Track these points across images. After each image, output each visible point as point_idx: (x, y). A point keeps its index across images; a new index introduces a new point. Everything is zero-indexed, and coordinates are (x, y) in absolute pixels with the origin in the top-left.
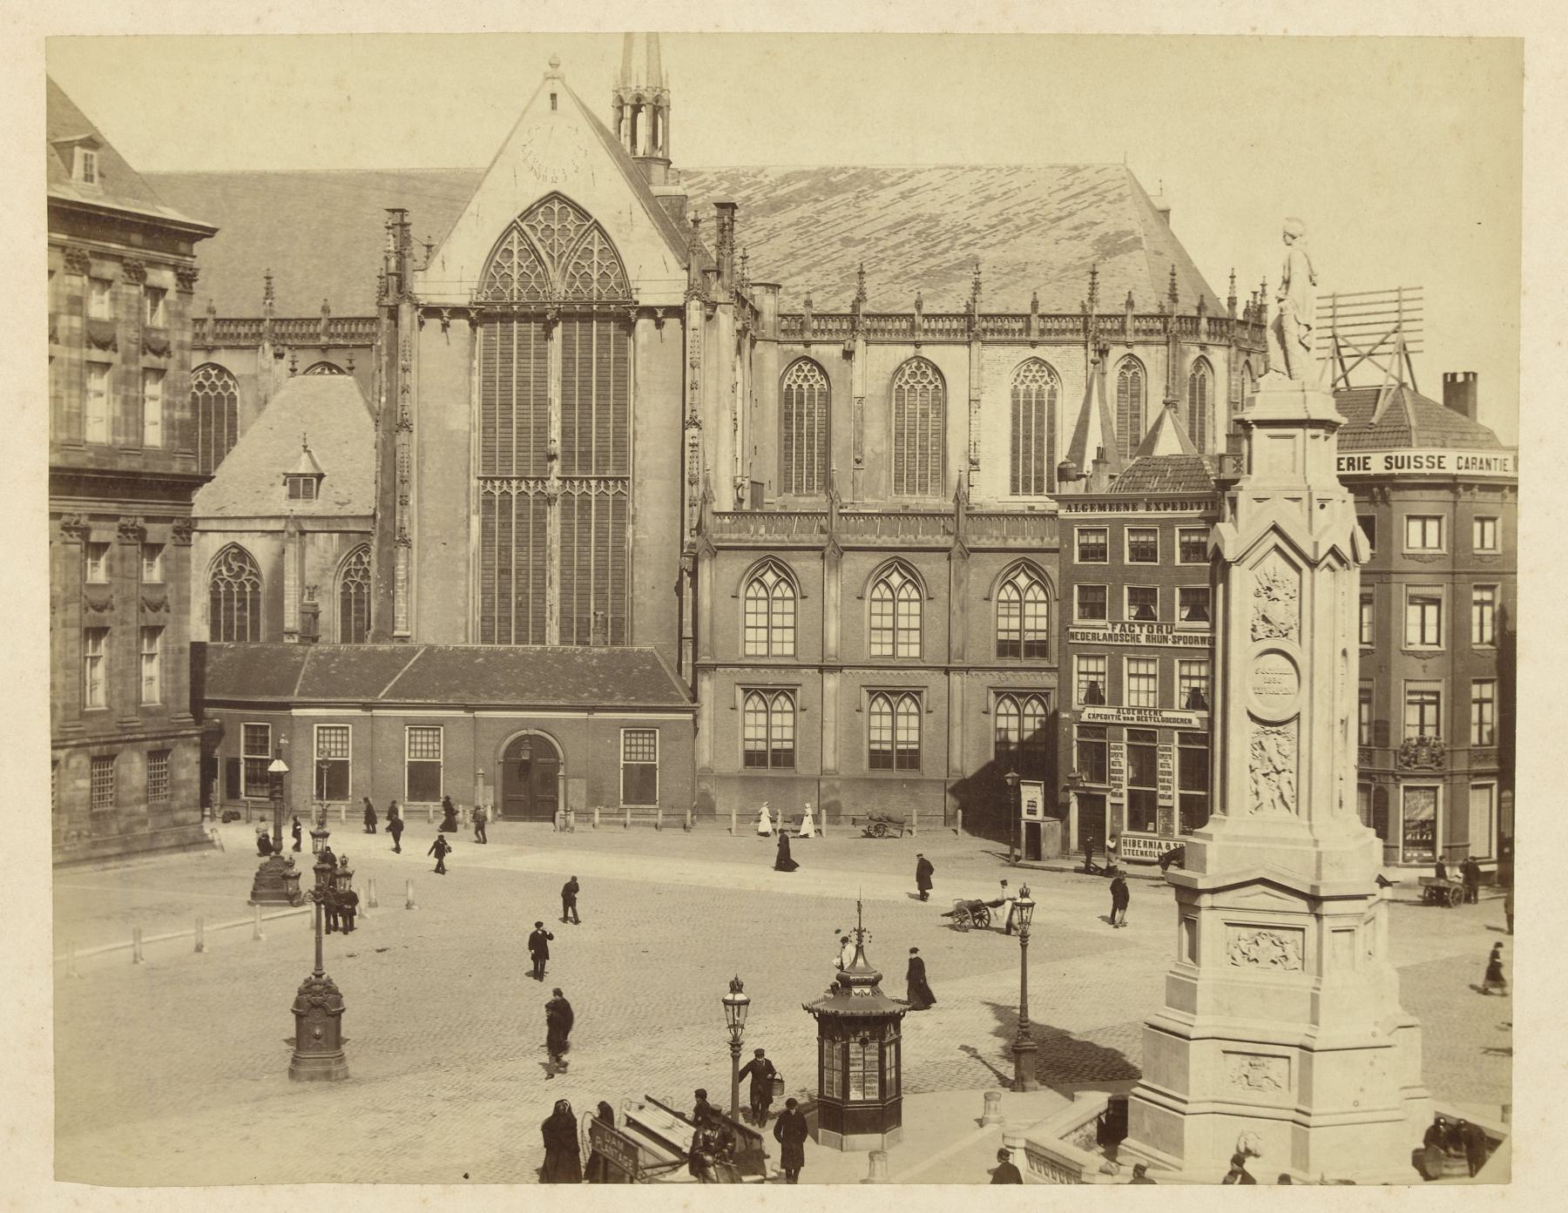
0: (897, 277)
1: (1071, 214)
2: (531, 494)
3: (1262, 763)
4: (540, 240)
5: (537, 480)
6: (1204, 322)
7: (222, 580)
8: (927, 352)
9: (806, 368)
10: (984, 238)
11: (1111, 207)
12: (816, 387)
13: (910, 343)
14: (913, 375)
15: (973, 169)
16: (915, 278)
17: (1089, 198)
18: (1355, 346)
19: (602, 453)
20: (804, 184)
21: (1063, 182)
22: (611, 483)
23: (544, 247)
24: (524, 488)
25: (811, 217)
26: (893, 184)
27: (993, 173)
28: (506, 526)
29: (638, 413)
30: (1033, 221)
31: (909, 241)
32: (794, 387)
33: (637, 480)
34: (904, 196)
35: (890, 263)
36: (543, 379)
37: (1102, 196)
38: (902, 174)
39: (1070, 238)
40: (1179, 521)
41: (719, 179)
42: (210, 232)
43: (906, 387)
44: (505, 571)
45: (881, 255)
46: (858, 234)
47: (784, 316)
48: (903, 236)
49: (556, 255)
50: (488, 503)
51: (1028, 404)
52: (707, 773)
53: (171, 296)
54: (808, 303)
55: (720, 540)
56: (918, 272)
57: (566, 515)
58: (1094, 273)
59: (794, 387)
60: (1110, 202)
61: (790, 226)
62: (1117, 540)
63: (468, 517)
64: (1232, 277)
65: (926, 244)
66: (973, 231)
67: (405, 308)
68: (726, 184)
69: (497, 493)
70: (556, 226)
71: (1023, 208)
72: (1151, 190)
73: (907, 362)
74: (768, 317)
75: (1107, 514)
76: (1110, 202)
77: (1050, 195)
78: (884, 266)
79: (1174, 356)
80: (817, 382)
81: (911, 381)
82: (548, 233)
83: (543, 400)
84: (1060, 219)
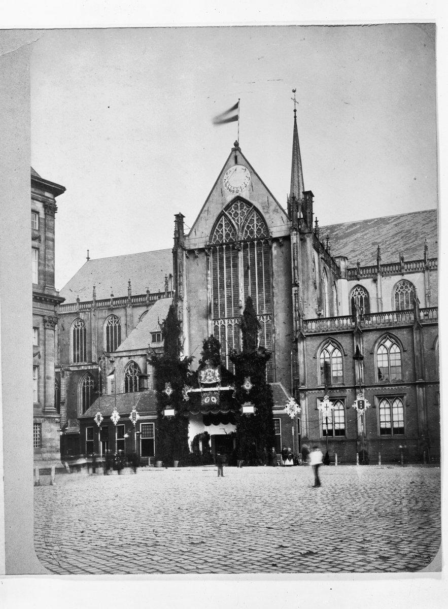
0: (395, 252)
4: (233, 218)
7: (129, 376)
9: (359, 290)
12: (363, 296)
23: (235, 221)
24: (230, 323)
26: (392, 222)
31: (398, 240)
41: (326, 230)
47: (349, 270)
49: (239, 224)
52: (306, 440)
65: (405, 240)
68: (329, 231)
69: (219, 326)
74: (343, 270)
78: (389, 250)
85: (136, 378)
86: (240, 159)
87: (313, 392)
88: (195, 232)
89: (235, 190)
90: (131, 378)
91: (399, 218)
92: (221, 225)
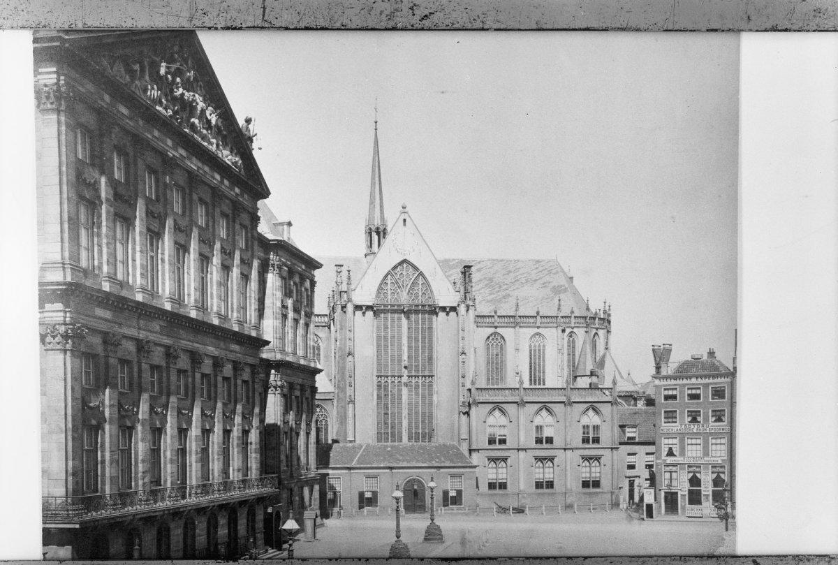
5: (398, 376)
8: (499, 330)
17: (546, 272)
19: (424, 366)
29: (438, 350)
31: (483, 288)
36: (400, 337)
37: (550, 272)
40: (711, 384)
44: (386, 414)
50: (379, 386)
62: (682, 392)
66: (506, 284)
72: (566, 270)
75: (678, 382)
83: (400, 345)
84: (536, 280)
91: (479, 263)
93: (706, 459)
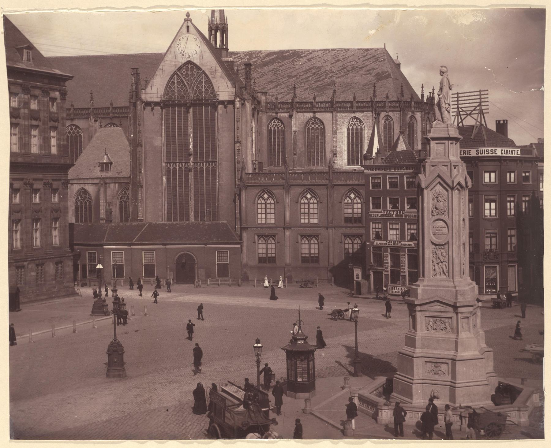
0: (307, 89)
1: (367, 66)
2: (183, 168)
3: (436, 259)
4: (184, 78)
5: (185, 163)
6: (413, 103)
8: (318, 115)
9: (276, 122)
10: (336, 74)
11: (380, 63)
12: (280, 128)
13: (312, 112)
14: (313, 124)
15: (333, 50)
16: (313, 89)
17: (372, 60)
18: (465, 111)
19: (207, 153)
20: (274, 56)
21: (364, 55)
22: (211, 163)
23: (186, 81)
25: (277, 68)
26: (305, 56)
27: (339, 52)
28: (175, 179)
29: (219, 138)
30: (353, 68)
31: (311, 76)
32: (273, 128)
33: (219, 162)
34: (309, 60)
35: (304, 84)
37: (377, 59)
38: (308, 52)
39: (366, 74)
41: (245, 55)
42: (71, 78)
43: (311, 128)
45: (301, 81)
46: (293, 74)
48: (309, 74)
49: (190, 83)
50: (168, 171)
51: (353, 133)
53: (59, 101)
54: (277, 99)
55: (248, 183)
56: (314, 87)
57: (196, 175)
58: (375, 87)
59: (273, 128)
60: (380, 62)
61: (270, 71)
63: (162, 177)
64: (422, 87)
67: (138, 103)
68: (248, 57)
70: (190, 73)
71: (349, 64)
72: (394, 57)
73: (311, 119)
74: (263, 104)
75: (381, 172)
76: (380, 62)
77: (359, 59)
78: (303, 85)
79: (403, 115)
80: (280, 126)
81: (313, 126)
82: (187, 75)
84: (362, 67)
85: (86, 203)
86: (192, 29)
87: (252, 229)
88: (151, 87)
89: (187, 55)
90: (81, 203)
91: (311, 53)
92: (174, 83)
93: (403, 243)
